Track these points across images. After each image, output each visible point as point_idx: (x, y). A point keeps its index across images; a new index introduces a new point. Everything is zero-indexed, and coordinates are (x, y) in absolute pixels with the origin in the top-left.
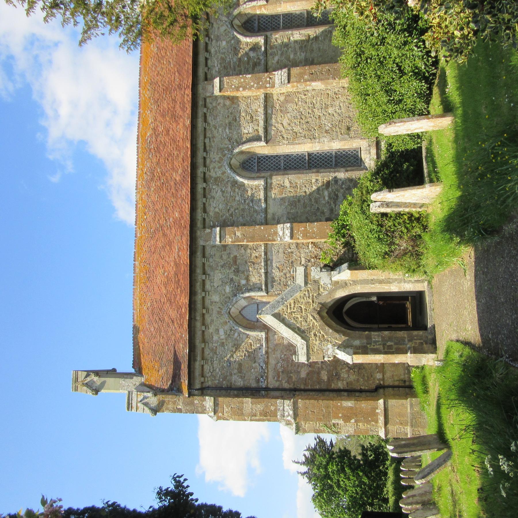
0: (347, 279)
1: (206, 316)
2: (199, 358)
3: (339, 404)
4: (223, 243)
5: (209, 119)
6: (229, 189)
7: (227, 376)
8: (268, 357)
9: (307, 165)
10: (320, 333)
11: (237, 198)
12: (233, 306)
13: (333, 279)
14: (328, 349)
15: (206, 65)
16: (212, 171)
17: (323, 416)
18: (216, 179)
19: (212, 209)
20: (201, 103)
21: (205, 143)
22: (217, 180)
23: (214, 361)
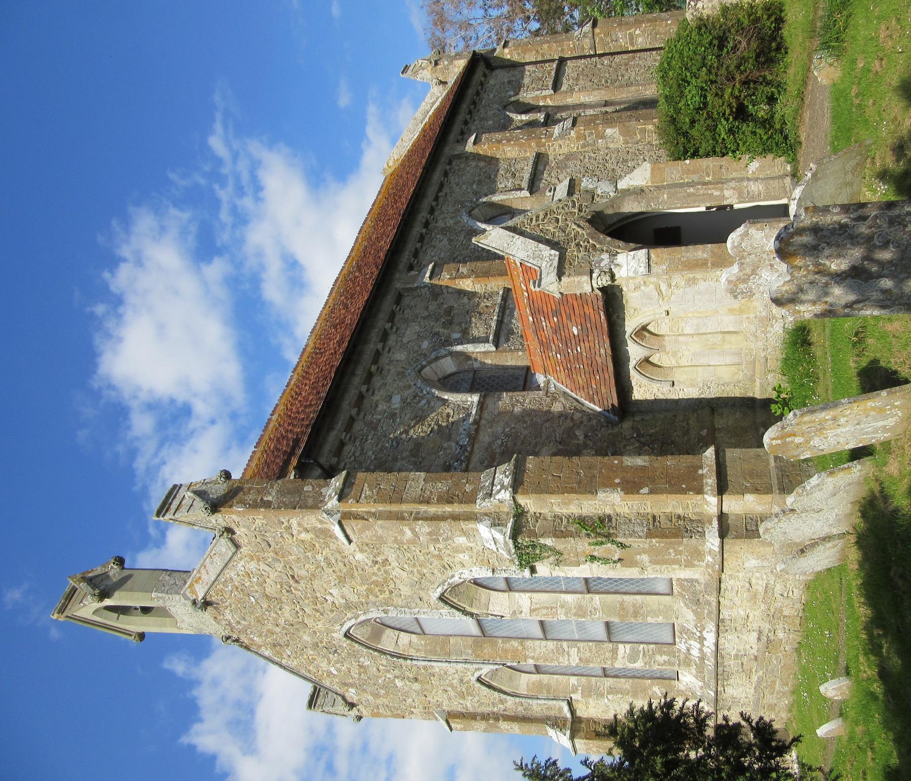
0: (644, 183)
2: (340, 425)
3: (616, 462)
4: (435, 281)
7: (386, 461)
8: (477, 431)
10: (588, 242)
12: (429, 363)
13: (619, 187)
14: (603, 260)
17: (579, 483)
23: (366, 440)
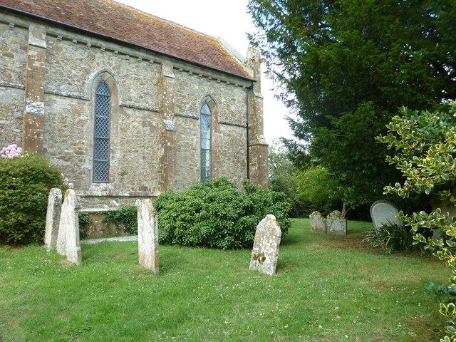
5: (144, 63)
6: (83, 66)
9: (98, 137)
11: (73, 71)
15: (184, 71)
16: (101, 55)
18: (94, 57)
19: (66, 46)
20: (158, 59)
21: (125, 54)
22: (92, 58)
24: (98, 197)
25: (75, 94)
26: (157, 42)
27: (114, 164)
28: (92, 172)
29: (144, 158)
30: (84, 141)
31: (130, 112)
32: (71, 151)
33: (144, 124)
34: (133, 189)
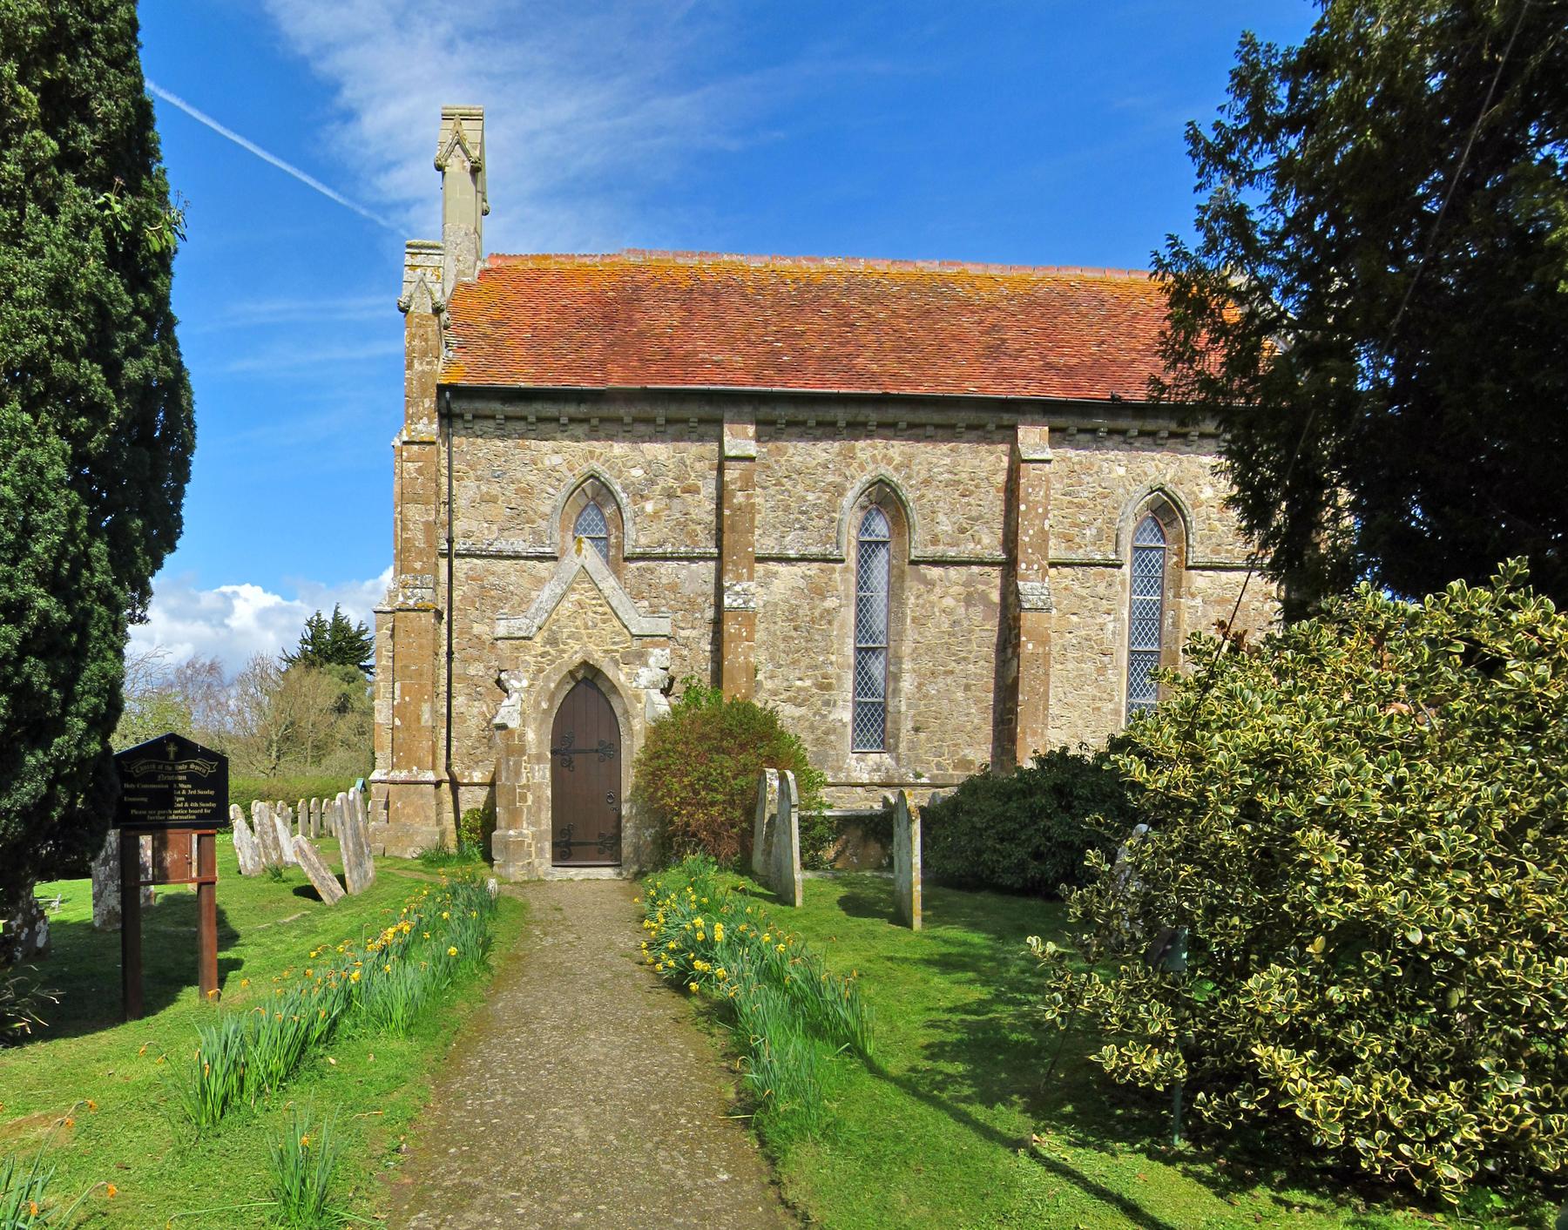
1: (586, 427)
6: (830, 478)
11: (811, 497)
21: (923, 426)
22: (850, 456)
24: (862, 785)
25: (815, 550)
26: (1007, 362)
27: (904, 704)
28: (850, 729)
29: (967, 688)
30: (833, 658)
31: (935, 572)
32: (808, 683)
33: (969, 601)
34: (939, 766)
